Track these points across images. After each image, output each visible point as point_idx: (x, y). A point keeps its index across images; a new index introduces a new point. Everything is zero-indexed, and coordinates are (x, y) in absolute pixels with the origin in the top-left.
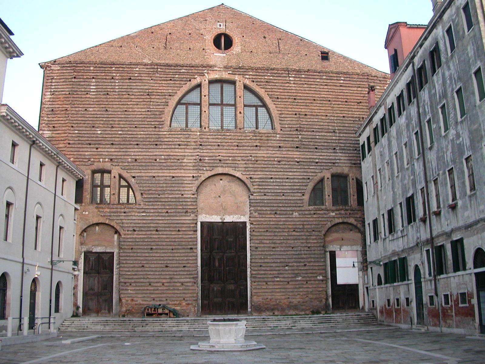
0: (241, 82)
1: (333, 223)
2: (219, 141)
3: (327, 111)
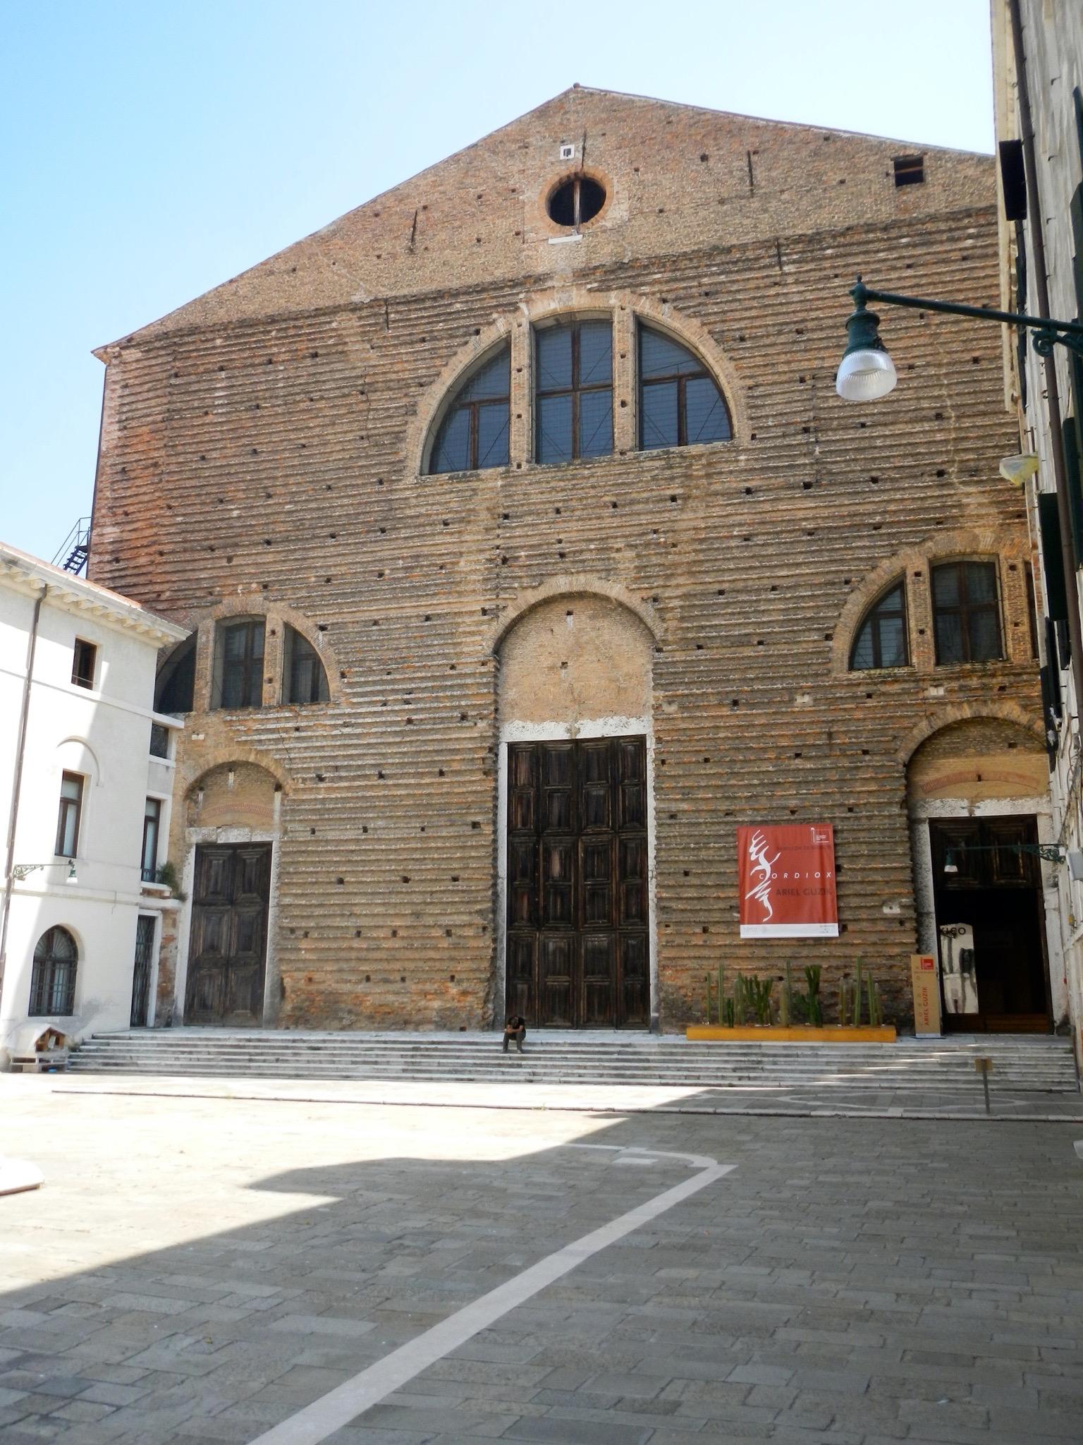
0: (628, 310)
1: (939, 724)
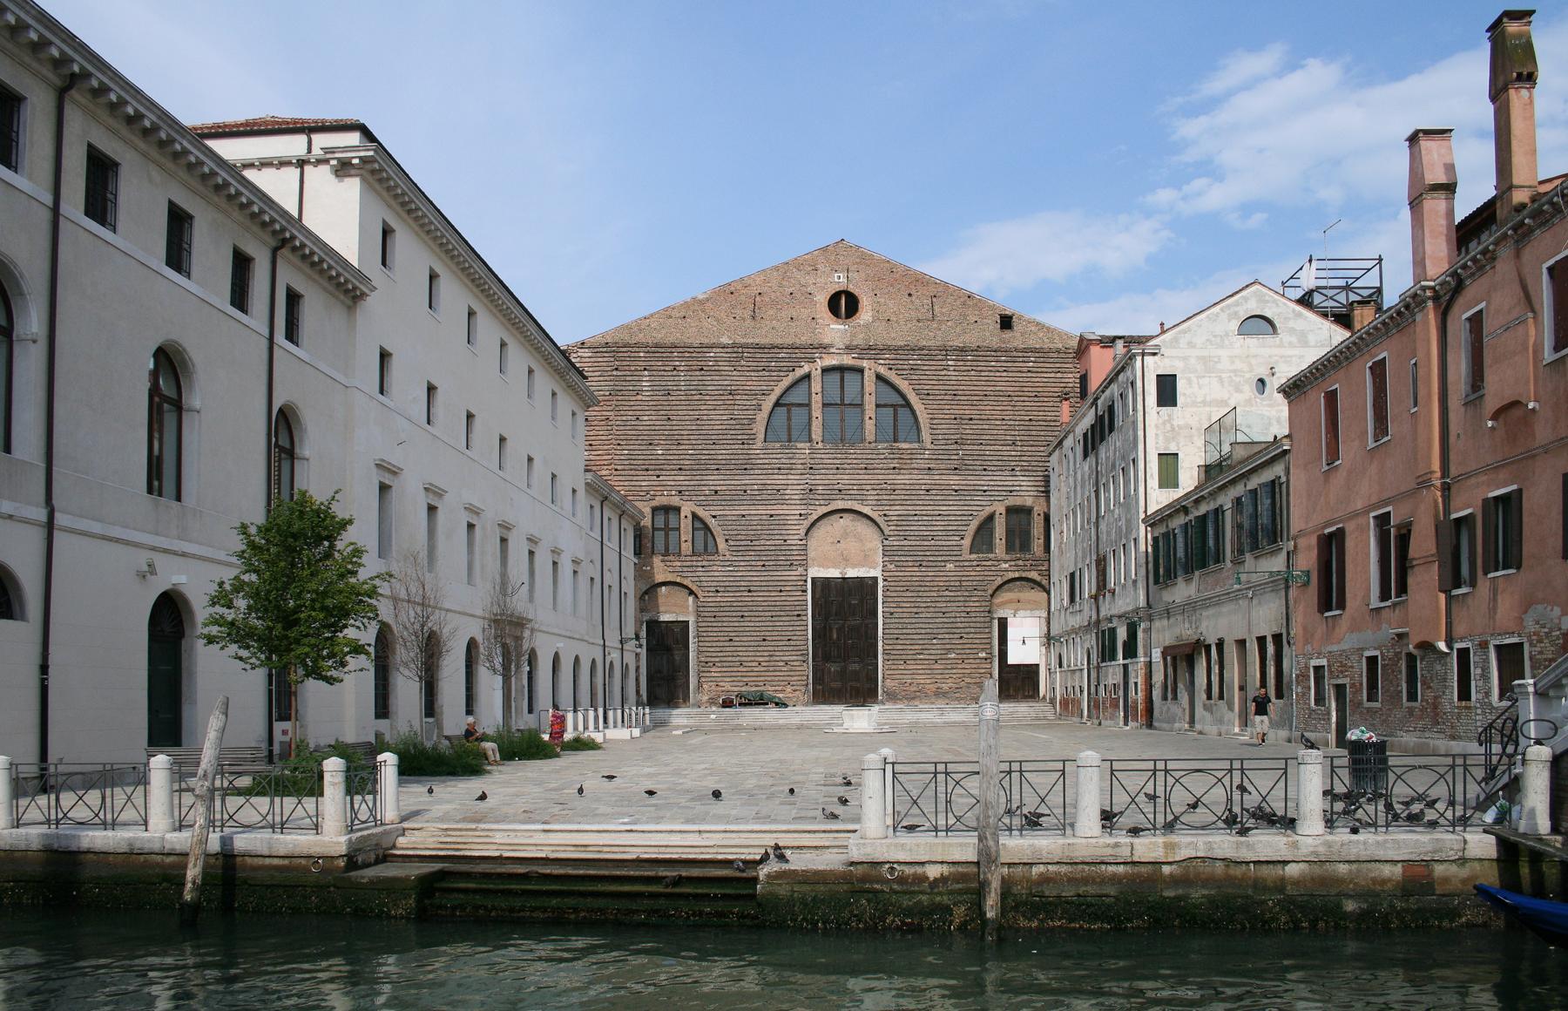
2: (838, 462)
3: (1005, 413)
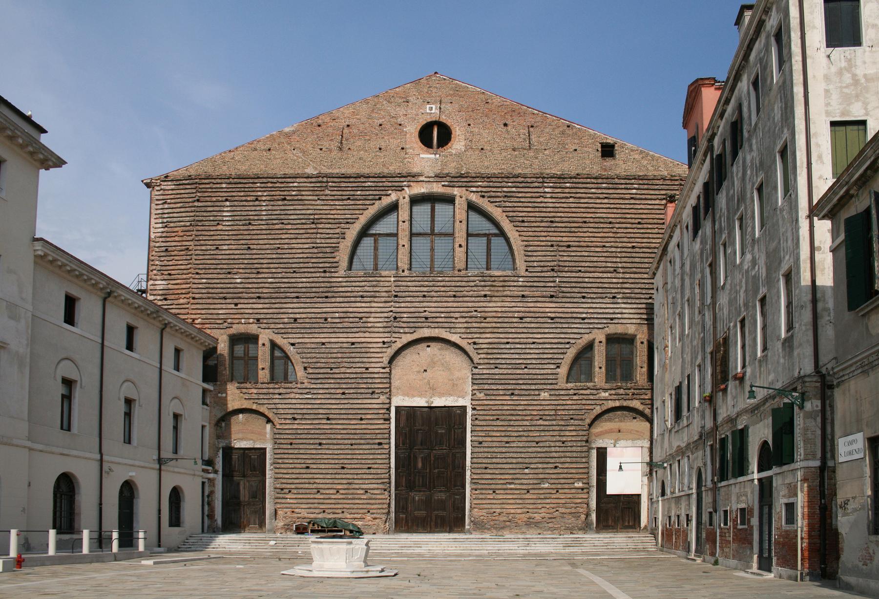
2: (425, 289)
